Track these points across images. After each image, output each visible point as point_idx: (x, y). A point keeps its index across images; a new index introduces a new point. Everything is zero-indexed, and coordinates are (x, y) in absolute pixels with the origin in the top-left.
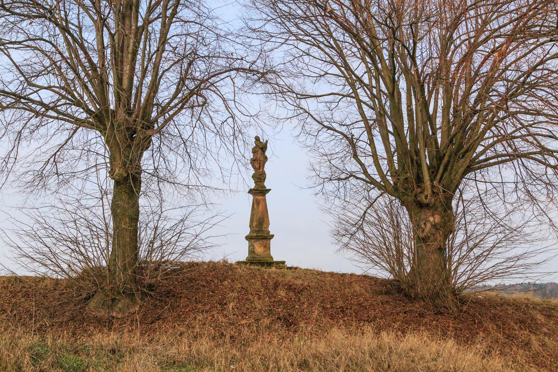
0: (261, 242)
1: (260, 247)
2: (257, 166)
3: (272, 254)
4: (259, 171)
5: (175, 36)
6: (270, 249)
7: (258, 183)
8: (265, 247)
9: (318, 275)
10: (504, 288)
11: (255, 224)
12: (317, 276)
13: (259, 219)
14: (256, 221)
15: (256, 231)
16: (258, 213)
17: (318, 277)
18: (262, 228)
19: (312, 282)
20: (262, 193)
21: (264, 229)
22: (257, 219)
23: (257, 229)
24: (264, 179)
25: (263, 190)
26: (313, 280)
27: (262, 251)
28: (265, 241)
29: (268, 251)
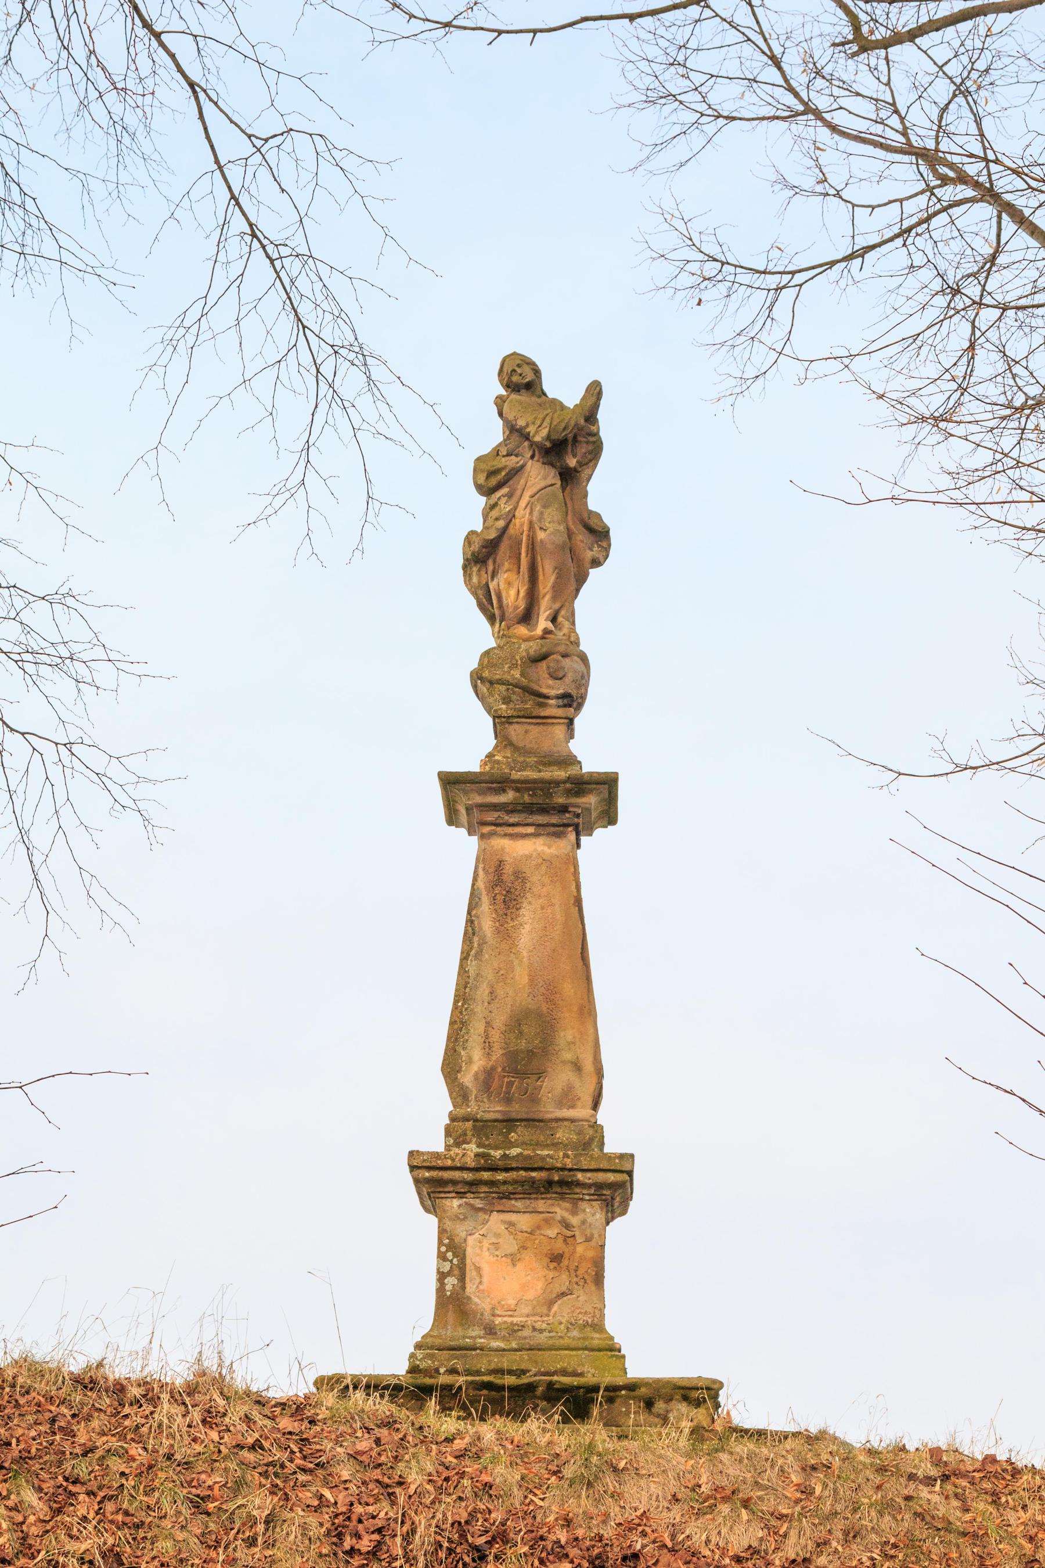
0: (524, 1221)
1: (514, 1259)
2: (513, 595)
3: (615, 1325)
4: (522, 630)
5: (843, 200)
6: (599, 1279)
7: (515, 731)
8: (556, 1258)
9: (930, 1481)
10: (521, 478)
11: (476, 1061)
12: (924, 1492)
13: (517, 1023)
14: (487, 1046)
15: (481, 1127)
16: (504, 976)
17: (930, 1496)
18: (535, 1100)
19: (851, 1535)
20: (544, 810)
21: (551, 1111)
22: (500, 1020)
23: (493, 1110)
24: (573, 701)
25: (547, 786)
26: (868, 1519)
27: (536, 1289)
28: (560, 1210)
29: (582, 1297)
